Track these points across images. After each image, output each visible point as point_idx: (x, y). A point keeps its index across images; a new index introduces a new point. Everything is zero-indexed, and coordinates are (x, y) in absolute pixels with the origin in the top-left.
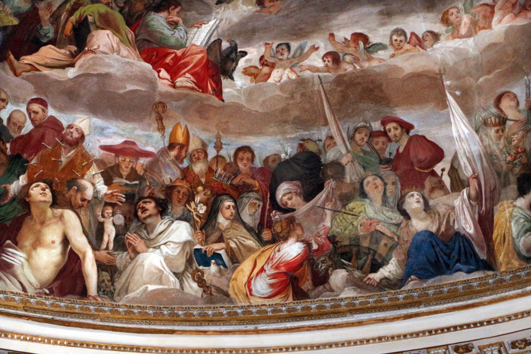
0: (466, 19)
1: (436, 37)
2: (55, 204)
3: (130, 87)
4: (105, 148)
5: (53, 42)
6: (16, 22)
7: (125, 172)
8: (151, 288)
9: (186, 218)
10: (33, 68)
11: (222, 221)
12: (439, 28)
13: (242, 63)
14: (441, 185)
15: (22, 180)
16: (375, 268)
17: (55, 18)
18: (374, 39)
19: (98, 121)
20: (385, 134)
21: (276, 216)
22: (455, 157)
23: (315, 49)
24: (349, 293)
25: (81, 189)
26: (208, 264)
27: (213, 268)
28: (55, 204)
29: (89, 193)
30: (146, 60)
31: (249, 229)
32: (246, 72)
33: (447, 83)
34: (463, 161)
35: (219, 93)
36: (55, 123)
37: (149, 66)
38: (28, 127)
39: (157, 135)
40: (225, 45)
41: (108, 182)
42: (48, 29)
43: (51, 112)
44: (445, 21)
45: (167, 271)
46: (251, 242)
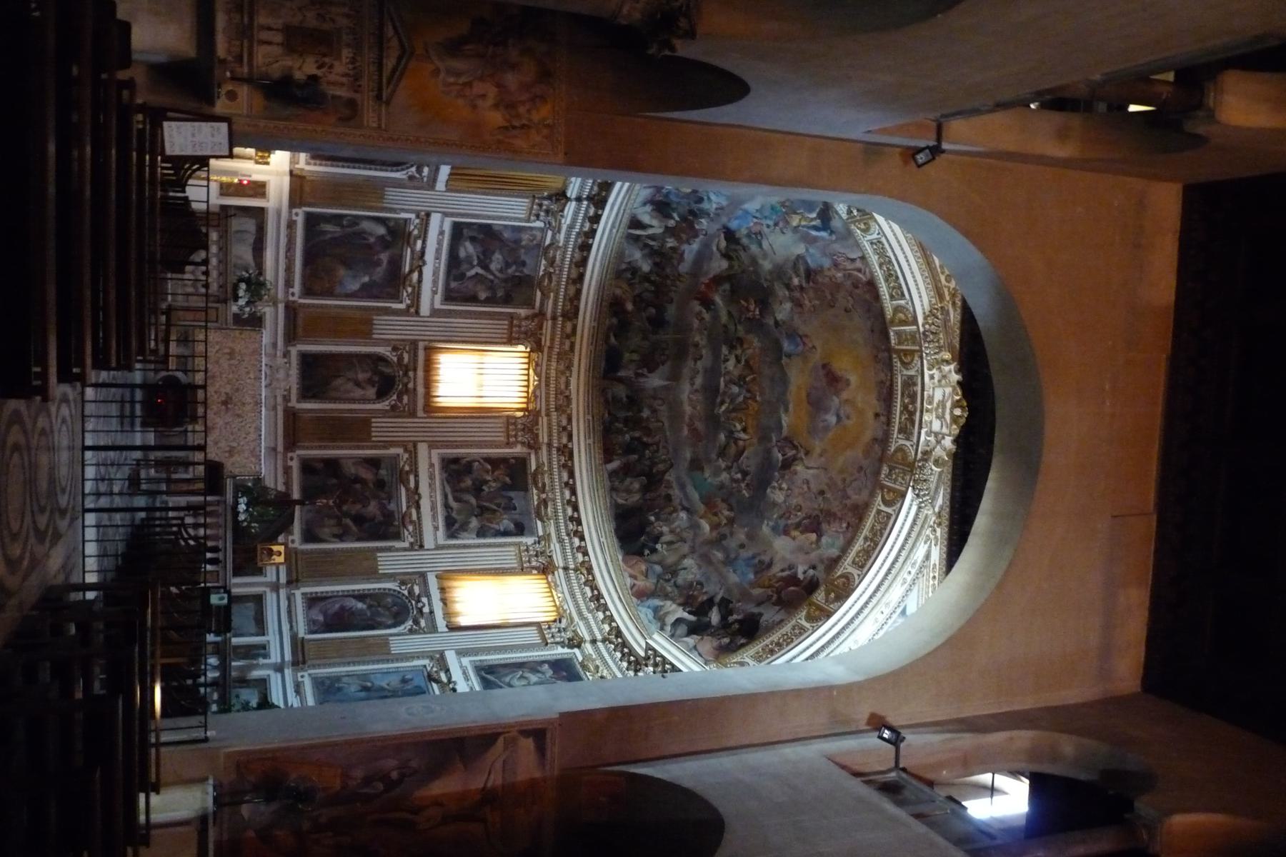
0: (695, 398)
1: (692, 384)
2: (667, 227)
3: (705, 267)
4: (684, 252)
5: (727, 247)
6: (737, 236)
7: (675, 255)
8: (627, 252)
9: (651, 272)
10: (719, 236)
11: (647, 285)
12: (695, 387)
13: (704, 311)
14: (638, 369)
15: (677, 219)
16: (615, 336)
17: (736, 250)
18: (699, 363)
19: (694, 252)
20: (664, 355)
21: (644, 305)
22: (647, 377)
23: (702, 339)
24: (607, 322)
25: (670, 237)
26: (632, 274)
27: (629, 276)
28: (667, 227)
29: (668, 240)
30: (715, 277)
31: (641, 293)
32: (701, 312)
33: (674, 383)
34: (646, 380)
35: (697, 299)
36: (696, 236)
37: (711, 276)
38: (697, 227)
39: (685, 270)
40: (713, 307)
41: (671, 248)
42: (733, 247)
43: (701, 237)
44: (697, 391)
45: (631, 259)
46: (637, 292)
